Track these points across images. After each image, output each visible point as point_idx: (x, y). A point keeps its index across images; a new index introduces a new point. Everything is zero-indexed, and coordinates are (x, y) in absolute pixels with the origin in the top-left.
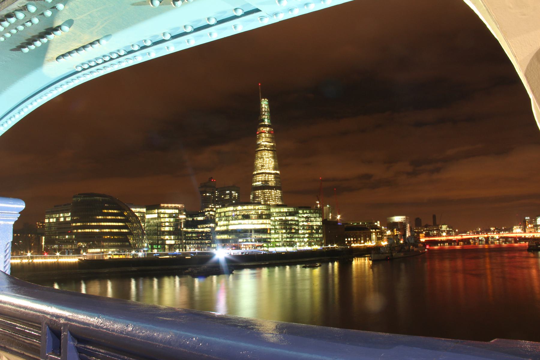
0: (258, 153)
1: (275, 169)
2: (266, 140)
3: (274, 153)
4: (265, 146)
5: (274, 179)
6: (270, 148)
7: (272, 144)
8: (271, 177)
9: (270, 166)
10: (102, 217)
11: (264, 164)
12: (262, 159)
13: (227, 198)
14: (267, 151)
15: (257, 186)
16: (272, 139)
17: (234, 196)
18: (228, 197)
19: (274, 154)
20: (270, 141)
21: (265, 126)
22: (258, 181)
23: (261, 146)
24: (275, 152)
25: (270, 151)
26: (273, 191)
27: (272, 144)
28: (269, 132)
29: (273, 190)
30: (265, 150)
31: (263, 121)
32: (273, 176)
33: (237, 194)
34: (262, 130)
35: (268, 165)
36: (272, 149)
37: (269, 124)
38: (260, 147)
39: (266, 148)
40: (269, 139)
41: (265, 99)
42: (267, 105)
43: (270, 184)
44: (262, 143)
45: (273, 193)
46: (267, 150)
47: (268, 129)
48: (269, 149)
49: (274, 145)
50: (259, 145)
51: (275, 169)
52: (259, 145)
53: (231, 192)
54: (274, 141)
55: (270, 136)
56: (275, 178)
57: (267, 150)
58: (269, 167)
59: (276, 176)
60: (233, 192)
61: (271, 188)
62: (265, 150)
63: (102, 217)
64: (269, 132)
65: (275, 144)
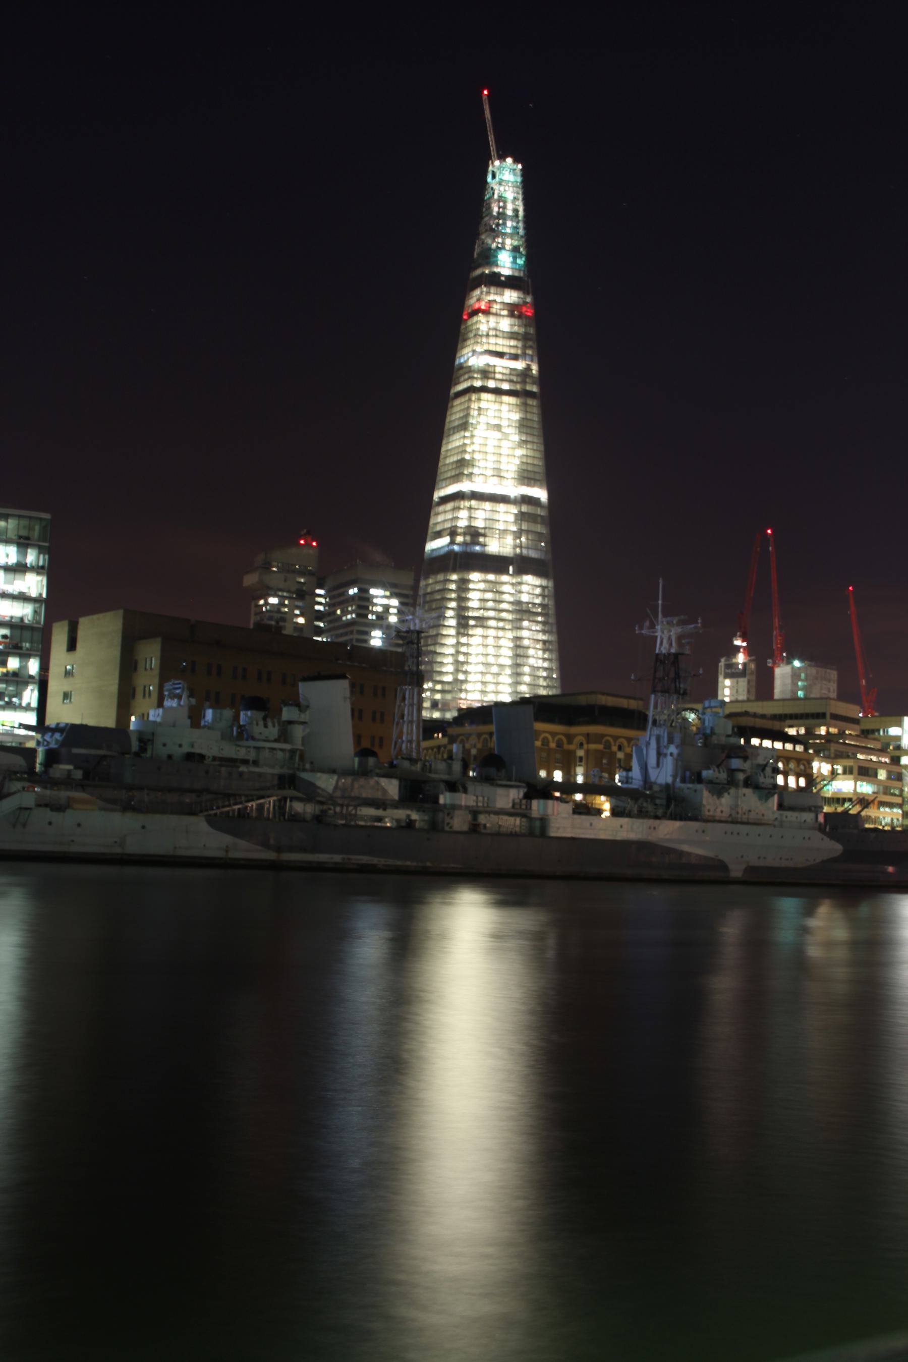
1: (525, 477)
2: (492, 348)
3: (525, 404)
5: (515, 522)
6: (511, 381)
7: (520, 365)
8: (506, 515)
9: (503, 467)
11: (477, 456)
13: (349, 617)
15: (436, 554)
16: (520, 344)
17: (379, 609)
18: (351, 613)
19: (524, 407)
20: (513, 351)
21: (496, 281)
22: (438, 535)
23: (465, 373)
24: (531, 402)
25: (506, 399)
26: (505, 578)
27: (520, 365)
28: (513, 310)
29: (507, 573)
30: (484, 389)
31: (489, 257)
32: (514, 509)
33: (395, 602)
35: (495, 458)
36: (519, 387)
38: (462, 379)
39: (491, 384)
40: (513, 343)
43: (494, 546)
45: (506, 588)
46: (498, 392)
47: (511, 296)
48: (506, 386)
49: (528, 368)
51: (525, 477)
53: (364, 591)
54: (529, 352)
55: (516, 329)
56: (521, 517)
57: (498, 392)
58: (499, 469)
59: (524, 508)
60: (373, 591)
61: (497, 564)
62: (484, 389)
64: (513, 310)
65: (535, 369)
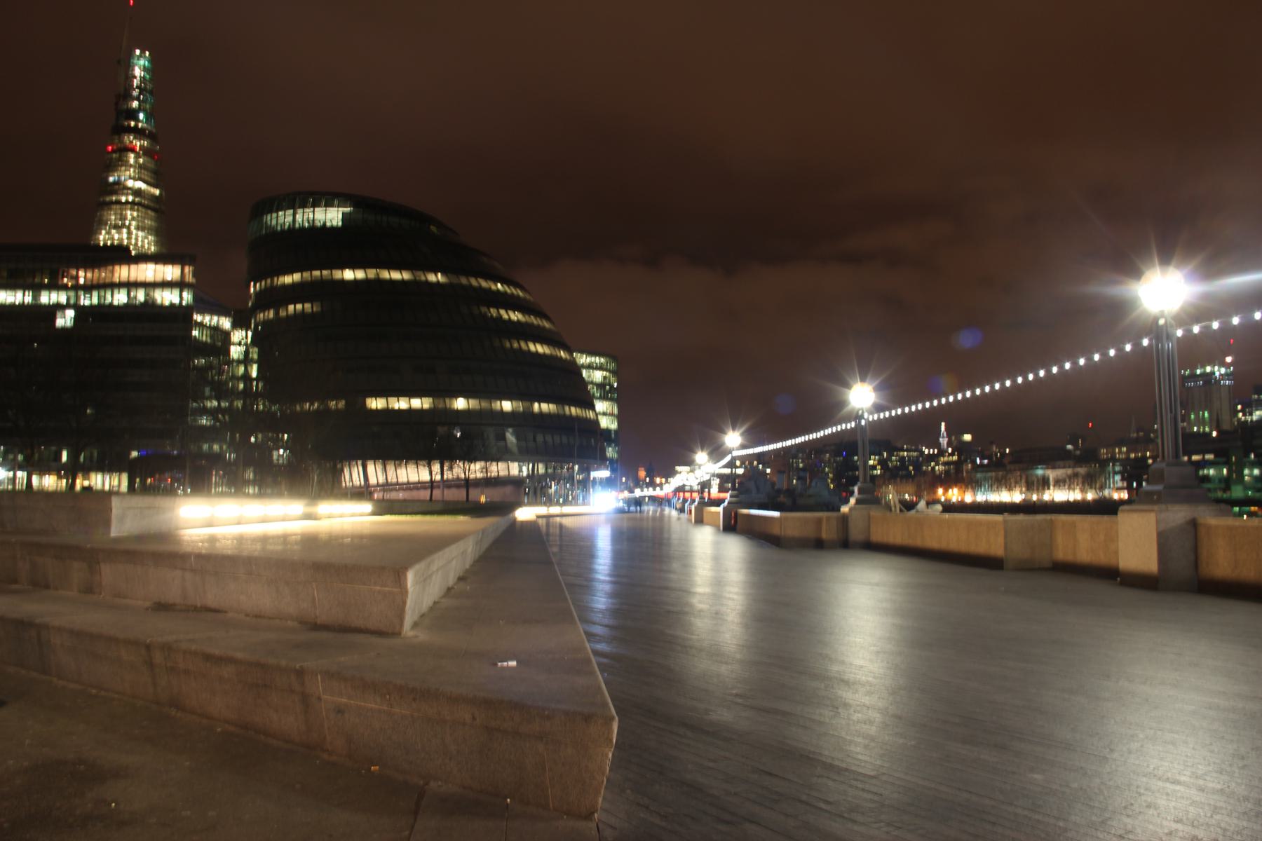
0: (111, 209)
4: (137, 193)
7: (157, 192)
10: (337, 274)
12: (125, 231)
14: (144, 210)
19: (157, 220)
21: (139, 133)
25: (149, 212)
27: (157, 192)
28: (146, 152)
34: (132, 142)
36: (157, 207)
37: (149, 128)
41: (143, 52)
42: (145, 69)
44: (130, 183)
46: (139, 204)
50: (119, 187)
52: (117, 187)
63: (337, 274)
64: (146, 152)
